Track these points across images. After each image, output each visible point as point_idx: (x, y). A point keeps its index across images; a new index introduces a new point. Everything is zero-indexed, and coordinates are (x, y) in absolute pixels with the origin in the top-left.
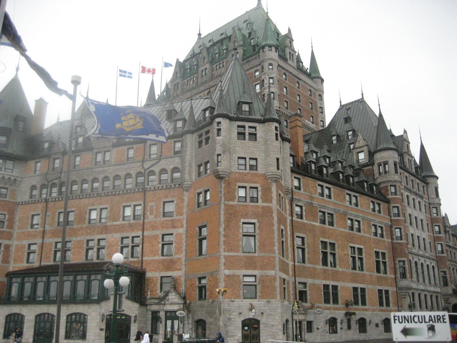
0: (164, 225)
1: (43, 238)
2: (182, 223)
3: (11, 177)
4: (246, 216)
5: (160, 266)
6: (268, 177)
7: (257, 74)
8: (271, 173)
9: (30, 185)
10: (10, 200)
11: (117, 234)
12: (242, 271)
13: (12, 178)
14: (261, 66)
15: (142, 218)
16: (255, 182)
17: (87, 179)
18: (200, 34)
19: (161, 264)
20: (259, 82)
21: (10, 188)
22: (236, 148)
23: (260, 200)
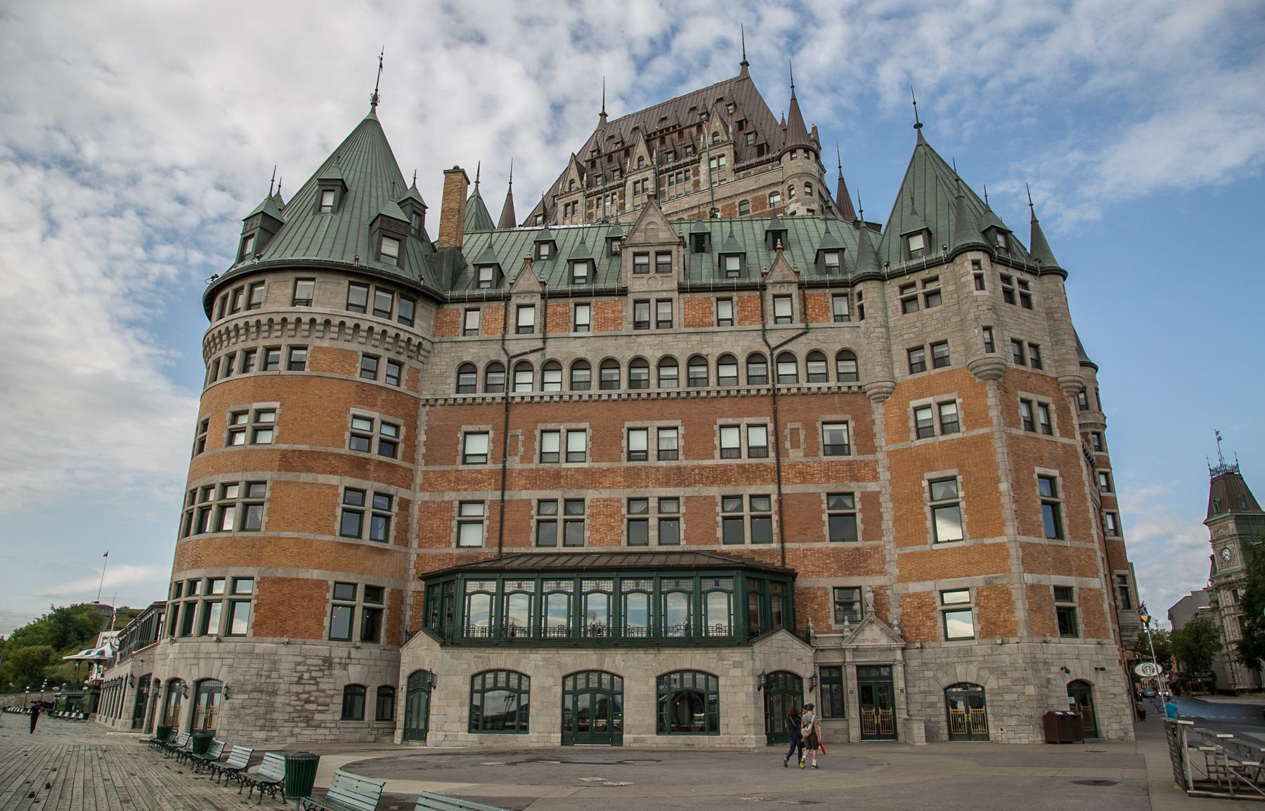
0: (828, 472)
1: (503, 490)
2: (874, 470)
3: (412, 337)
4: (1040, 461)
5: (830, 563)
6: (1062, 385)
7: (777, 198)
8: (1072, 378)
9: (458, 362)
10: (409, 393)
11: (710, 488)
12: (1053, 577)
13: (415, 341)
14: (785, 187)
15: (772, 454)
16: (1044, 394)
17: (618, 357)
18: (604, 115)
19: (833, 559)
21: (409, 364)
22: (1006, 319)
23: (1056, 431)
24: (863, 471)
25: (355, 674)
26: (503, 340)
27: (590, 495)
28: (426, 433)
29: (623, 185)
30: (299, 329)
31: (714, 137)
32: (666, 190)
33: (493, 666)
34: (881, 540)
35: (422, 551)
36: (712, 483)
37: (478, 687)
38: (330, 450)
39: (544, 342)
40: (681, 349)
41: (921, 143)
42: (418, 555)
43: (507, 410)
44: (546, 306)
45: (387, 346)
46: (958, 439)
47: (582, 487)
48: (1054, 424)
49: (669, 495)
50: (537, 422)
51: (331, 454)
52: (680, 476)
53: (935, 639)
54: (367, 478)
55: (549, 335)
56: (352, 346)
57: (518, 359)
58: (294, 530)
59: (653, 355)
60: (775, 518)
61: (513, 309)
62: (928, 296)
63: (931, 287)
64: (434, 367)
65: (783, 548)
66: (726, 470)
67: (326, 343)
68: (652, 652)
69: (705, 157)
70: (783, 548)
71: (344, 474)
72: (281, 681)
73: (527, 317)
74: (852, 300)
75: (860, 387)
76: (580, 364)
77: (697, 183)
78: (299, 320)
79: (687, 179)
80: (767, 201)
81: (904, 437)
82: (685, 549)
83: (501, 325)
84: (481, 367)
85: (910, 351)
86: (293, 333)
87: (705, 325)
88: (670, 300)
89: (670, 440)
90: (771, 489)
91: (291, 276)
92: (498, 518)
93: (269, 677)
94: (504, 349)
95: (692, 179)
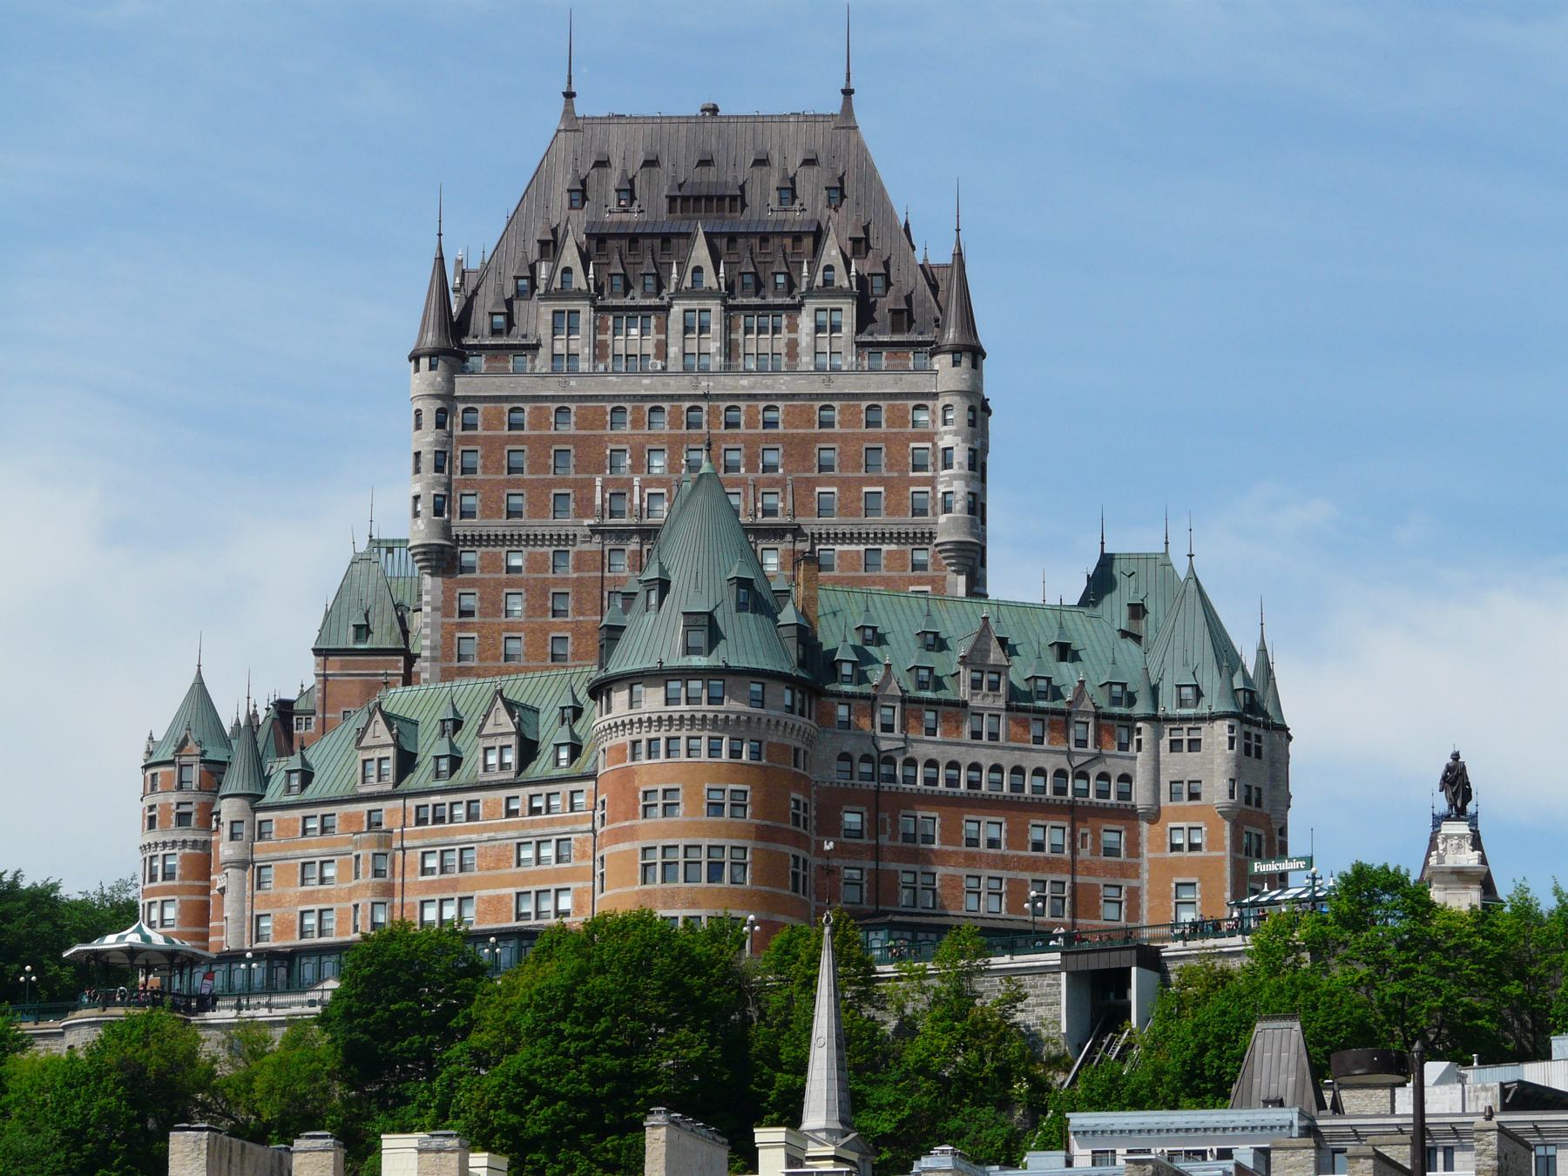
0: (1107, 870)
7: (923, 417)
15: (1067, 851)
20: (929, 445)
21: (810, 752)
29: (666, 309)
32: (741, 341)
40: (1008, 760)
48: (1263, 851)
52: (1004, 862)
54: (799, 847)
58: (769, 885)
59: (986, 763)
62: (1190, 741)
63: (1194, 735)
66: (1036, 860)
67: (774, 740)
69: (811, 305)
70: (1074, 925)
77: (793, 345)
79: (776, 330)
80: (910, 417)
81: (1161, 849)
84: (857, 757)
85: (1171, 783)
89: (994, 832)
90: (1067, 878)
95: (784, 335)
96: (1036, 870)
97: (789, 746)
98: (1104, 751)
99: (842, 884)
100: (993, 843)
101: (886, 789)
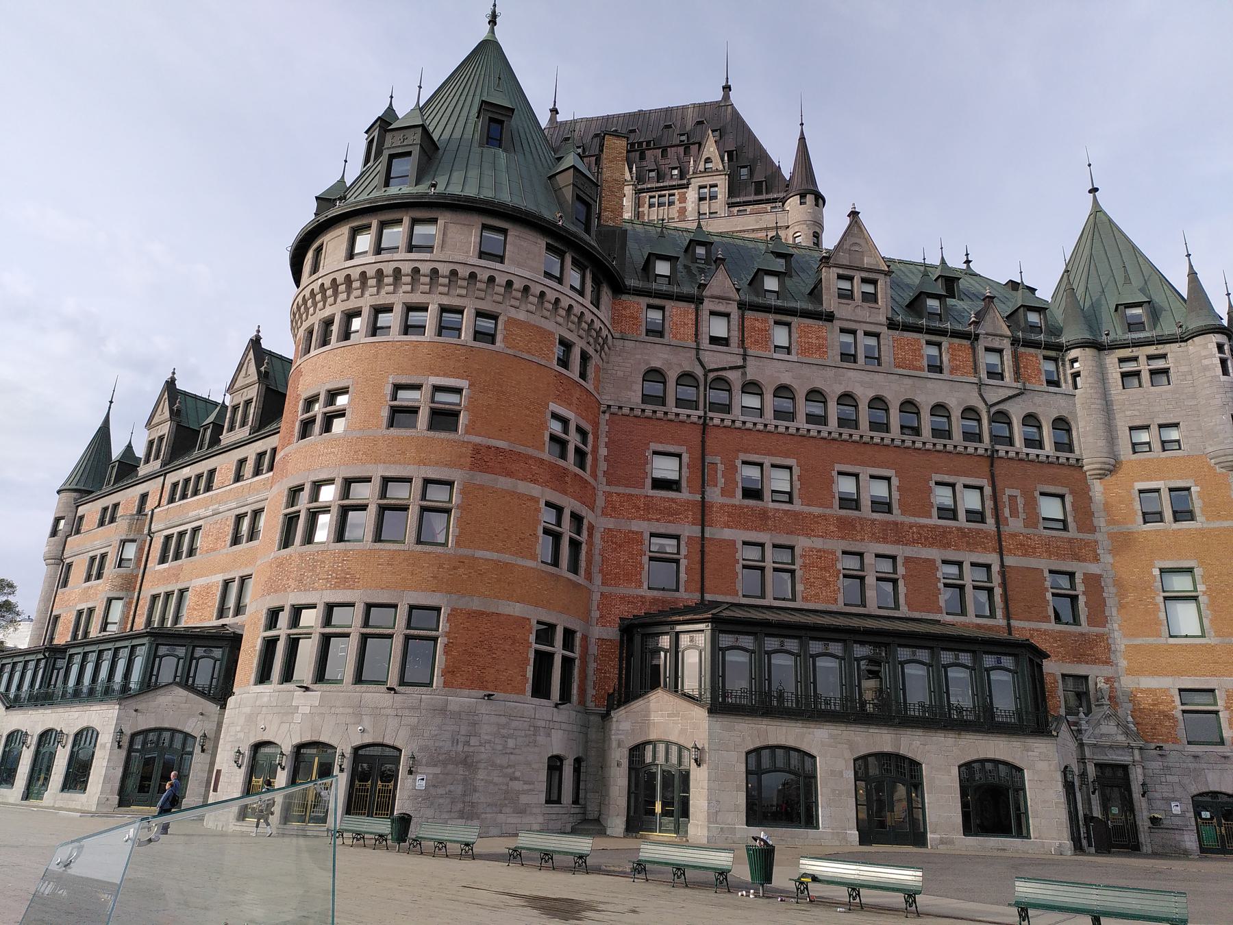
0: (1050, 549)
5: (1057, 647)
9: (644, 368)
15: (990, 521)
21: (595, 360)
24: (1083, 551)
25: (557, 743)
26: (698, 349)
27: (802, 543)
28: (607, 445)
30: (489, 291)
31: (706, 162)
32: (646, 212)
33: (772, 742)
34: (1105, 626)
35: (606, 589)
36: (932, 545)
37: (753, 767)
38: (531, 451)
39: (745, 360)
41: (1097, 210)
42: (602, 594)
43: (704, 433)
44: (742, 318)
45: (581, 332)
46: (1196, 529)
47: (792, 533)
49: (887, 553)
50: (739, 451)
51: (531, 457)
52: (897, 533)
53: (1175, 741)
54: (564, 492)
55: (750, 352)
56: (549, 325)
57: (716, 374)
58: (492, 550)
59: (864, 395)
60: (998, 591)
61: (705, 314)
62: (1153, 372)
63: (1160, 364)
64: (616, 368)
65: (1009, 625)
66: (945, 532)
67: (521, 316)
68: (951, 736)
69: (695, 183)
70: (1009, 625)
71: (545, 484)
72: (483, 749)
73: (719, 328)
74: (1063, 365)
75: (1078, 460)
76: (783, 391)
78: (492, 279)
79: (671, 204)
82: (907, 616)
83: (692, 331)
84: (672, 376)
86: (482, 294)
87: (916, 369)
88: (877, 335)
89: (879, 490)
90: (992, 559)
91: (478, 220)
92: (698, 558)
93: (467, 743)
94: (699, 360)
95: (677, 205)
96: (947, 546)
97: (552, 333)
98: (1028, 386)
99: (645, 559)
100: (882, 506)
101: (717, 421)
